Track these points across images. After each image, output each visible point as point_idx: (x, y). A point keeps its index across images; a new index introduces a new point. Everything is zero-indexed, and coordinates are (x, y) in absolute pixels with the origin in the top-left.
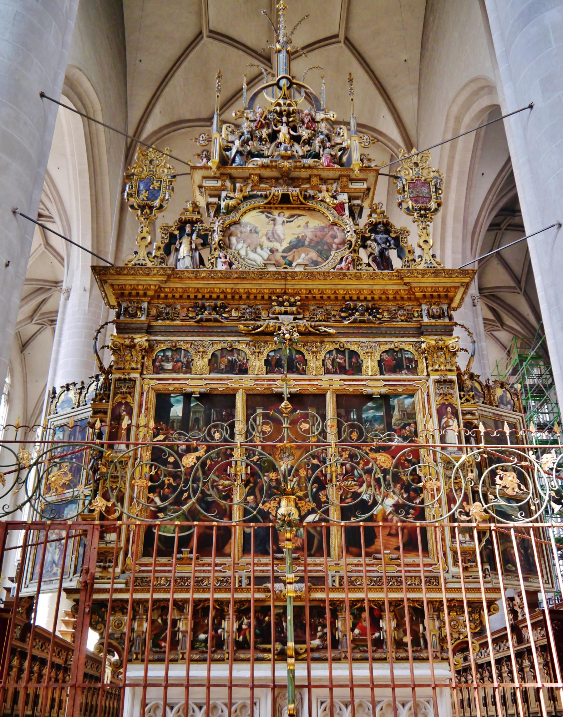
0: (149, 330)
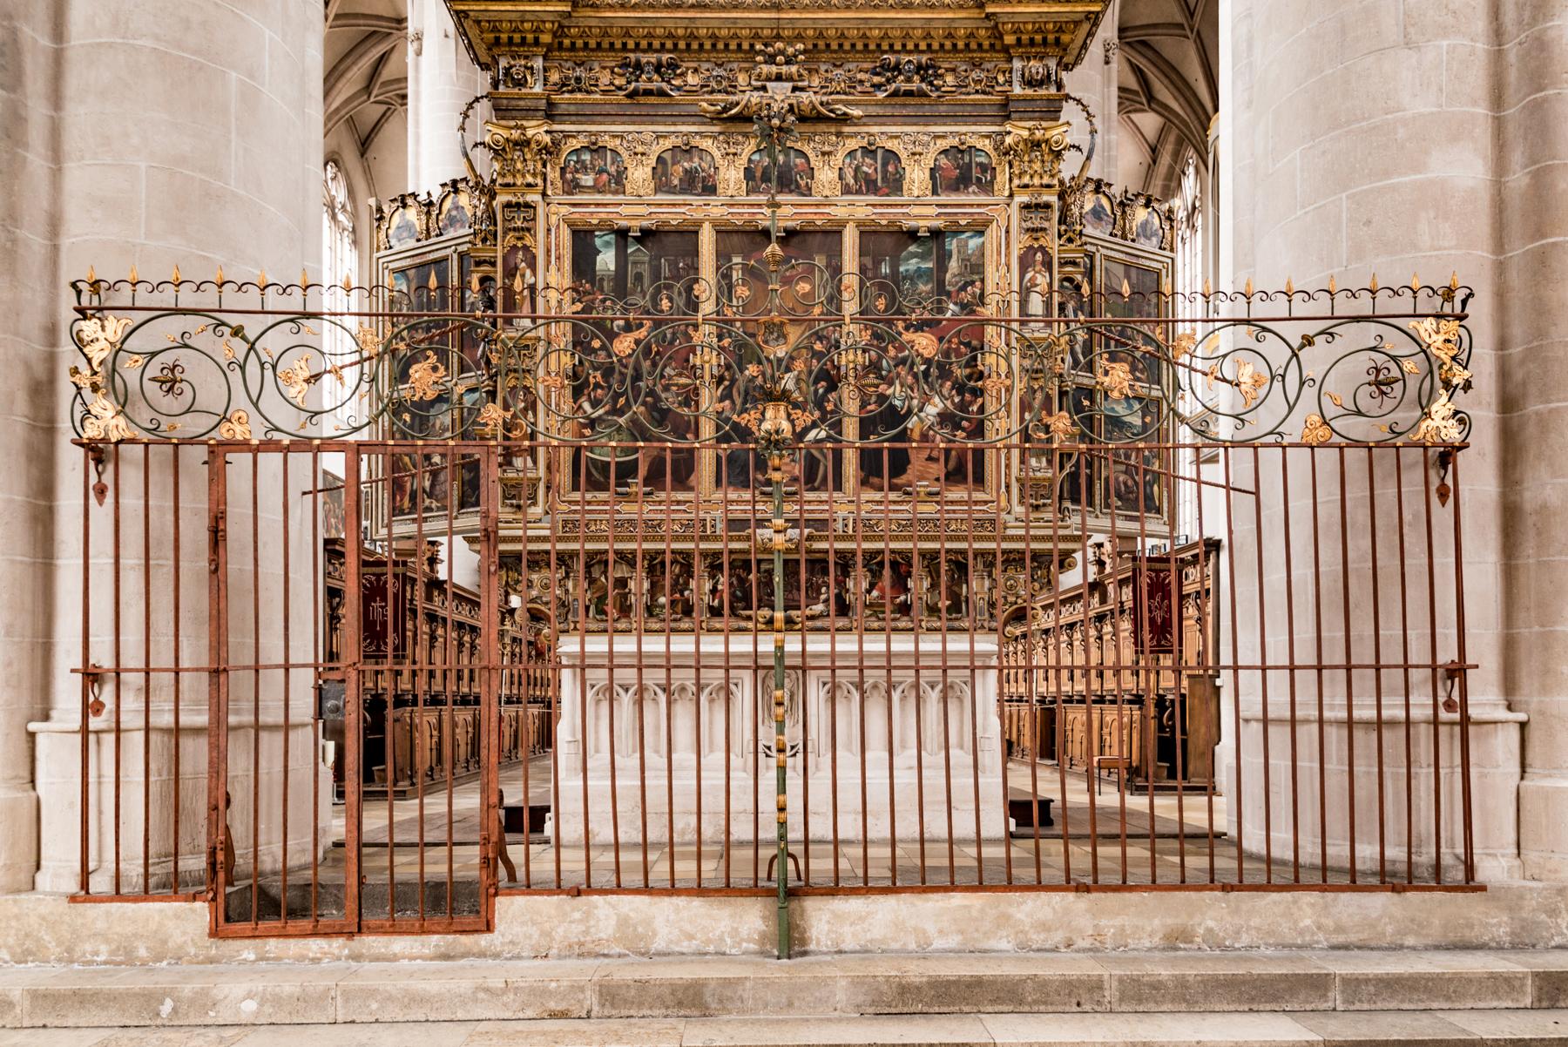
0: (550, 113)
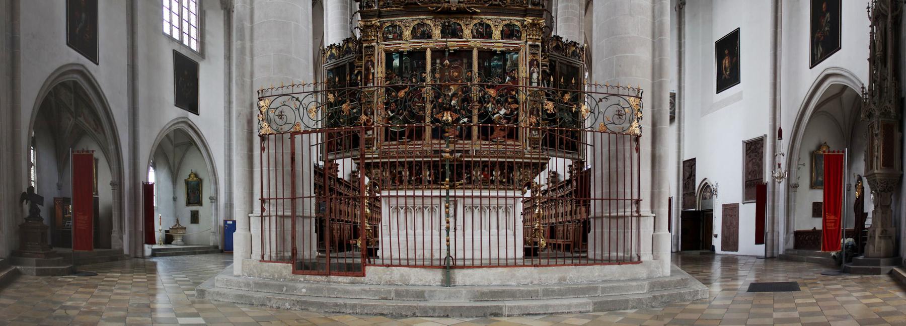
0: (380, 15)
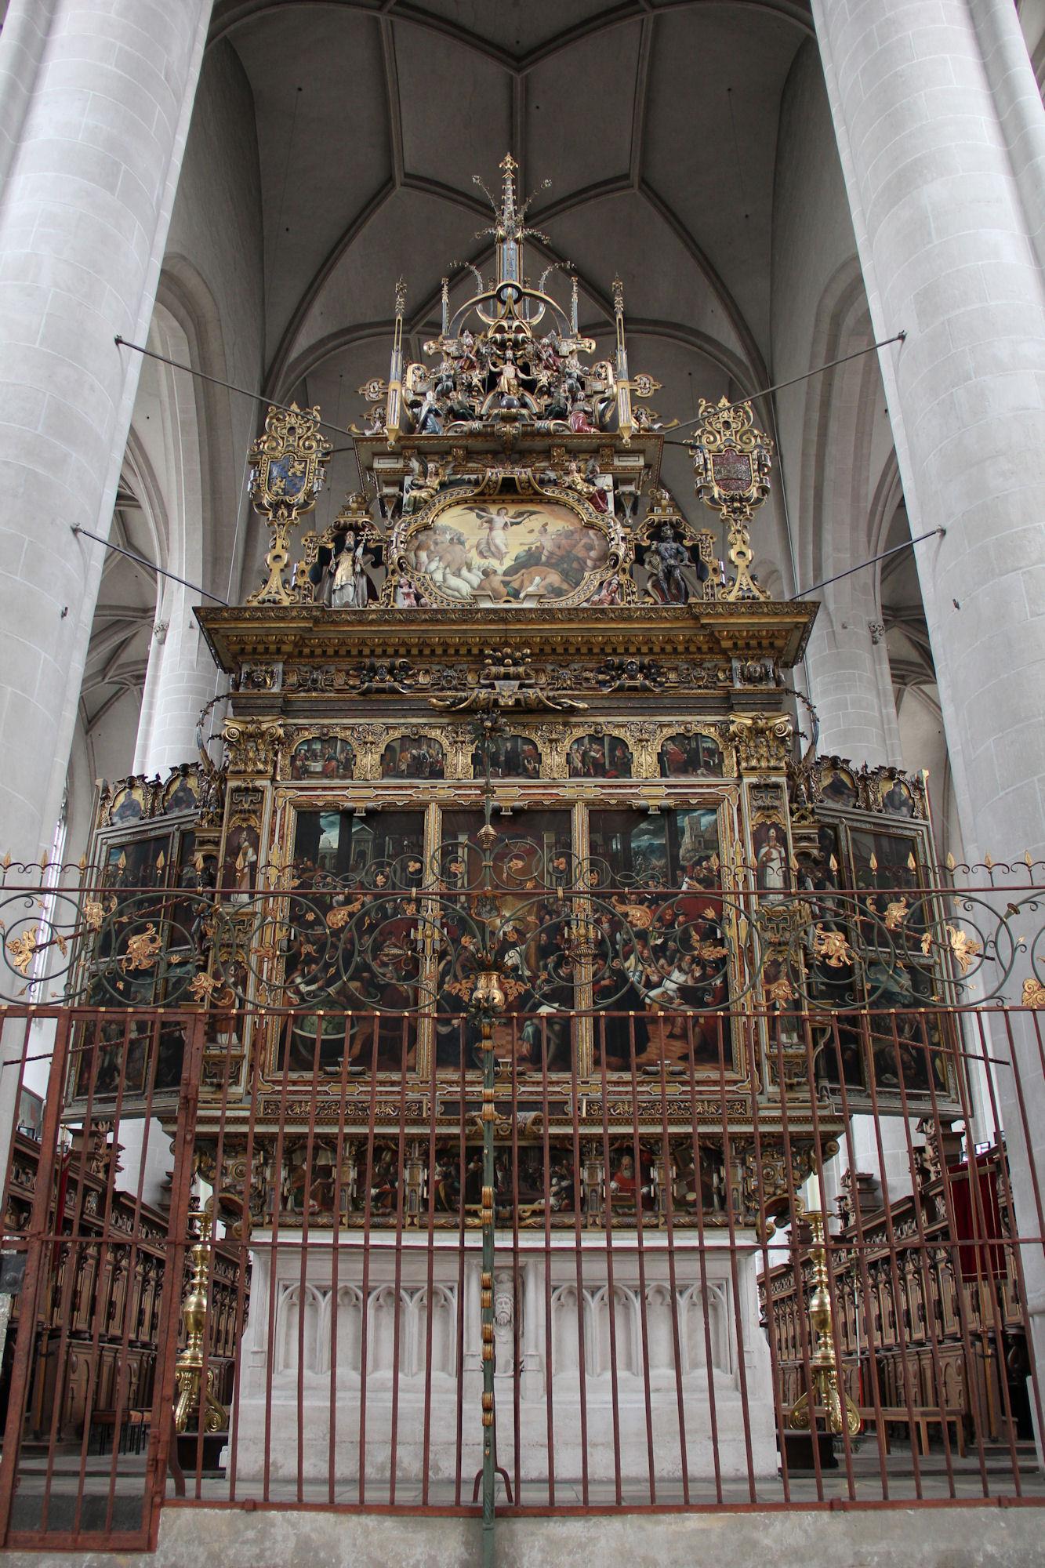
0: (286, 709)
